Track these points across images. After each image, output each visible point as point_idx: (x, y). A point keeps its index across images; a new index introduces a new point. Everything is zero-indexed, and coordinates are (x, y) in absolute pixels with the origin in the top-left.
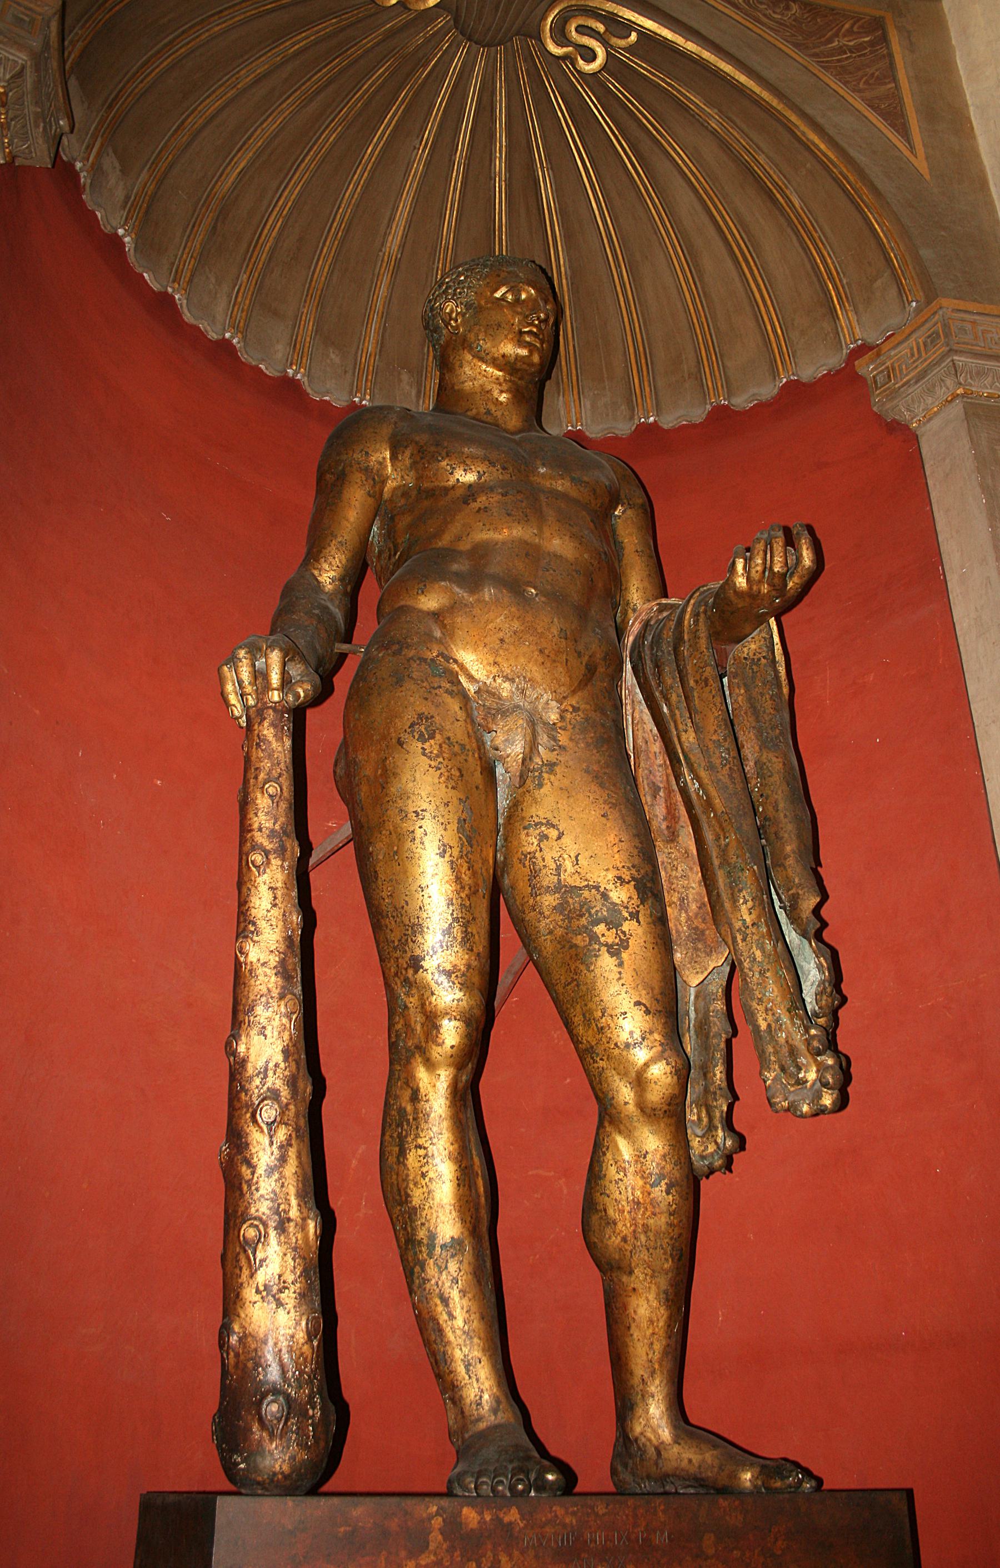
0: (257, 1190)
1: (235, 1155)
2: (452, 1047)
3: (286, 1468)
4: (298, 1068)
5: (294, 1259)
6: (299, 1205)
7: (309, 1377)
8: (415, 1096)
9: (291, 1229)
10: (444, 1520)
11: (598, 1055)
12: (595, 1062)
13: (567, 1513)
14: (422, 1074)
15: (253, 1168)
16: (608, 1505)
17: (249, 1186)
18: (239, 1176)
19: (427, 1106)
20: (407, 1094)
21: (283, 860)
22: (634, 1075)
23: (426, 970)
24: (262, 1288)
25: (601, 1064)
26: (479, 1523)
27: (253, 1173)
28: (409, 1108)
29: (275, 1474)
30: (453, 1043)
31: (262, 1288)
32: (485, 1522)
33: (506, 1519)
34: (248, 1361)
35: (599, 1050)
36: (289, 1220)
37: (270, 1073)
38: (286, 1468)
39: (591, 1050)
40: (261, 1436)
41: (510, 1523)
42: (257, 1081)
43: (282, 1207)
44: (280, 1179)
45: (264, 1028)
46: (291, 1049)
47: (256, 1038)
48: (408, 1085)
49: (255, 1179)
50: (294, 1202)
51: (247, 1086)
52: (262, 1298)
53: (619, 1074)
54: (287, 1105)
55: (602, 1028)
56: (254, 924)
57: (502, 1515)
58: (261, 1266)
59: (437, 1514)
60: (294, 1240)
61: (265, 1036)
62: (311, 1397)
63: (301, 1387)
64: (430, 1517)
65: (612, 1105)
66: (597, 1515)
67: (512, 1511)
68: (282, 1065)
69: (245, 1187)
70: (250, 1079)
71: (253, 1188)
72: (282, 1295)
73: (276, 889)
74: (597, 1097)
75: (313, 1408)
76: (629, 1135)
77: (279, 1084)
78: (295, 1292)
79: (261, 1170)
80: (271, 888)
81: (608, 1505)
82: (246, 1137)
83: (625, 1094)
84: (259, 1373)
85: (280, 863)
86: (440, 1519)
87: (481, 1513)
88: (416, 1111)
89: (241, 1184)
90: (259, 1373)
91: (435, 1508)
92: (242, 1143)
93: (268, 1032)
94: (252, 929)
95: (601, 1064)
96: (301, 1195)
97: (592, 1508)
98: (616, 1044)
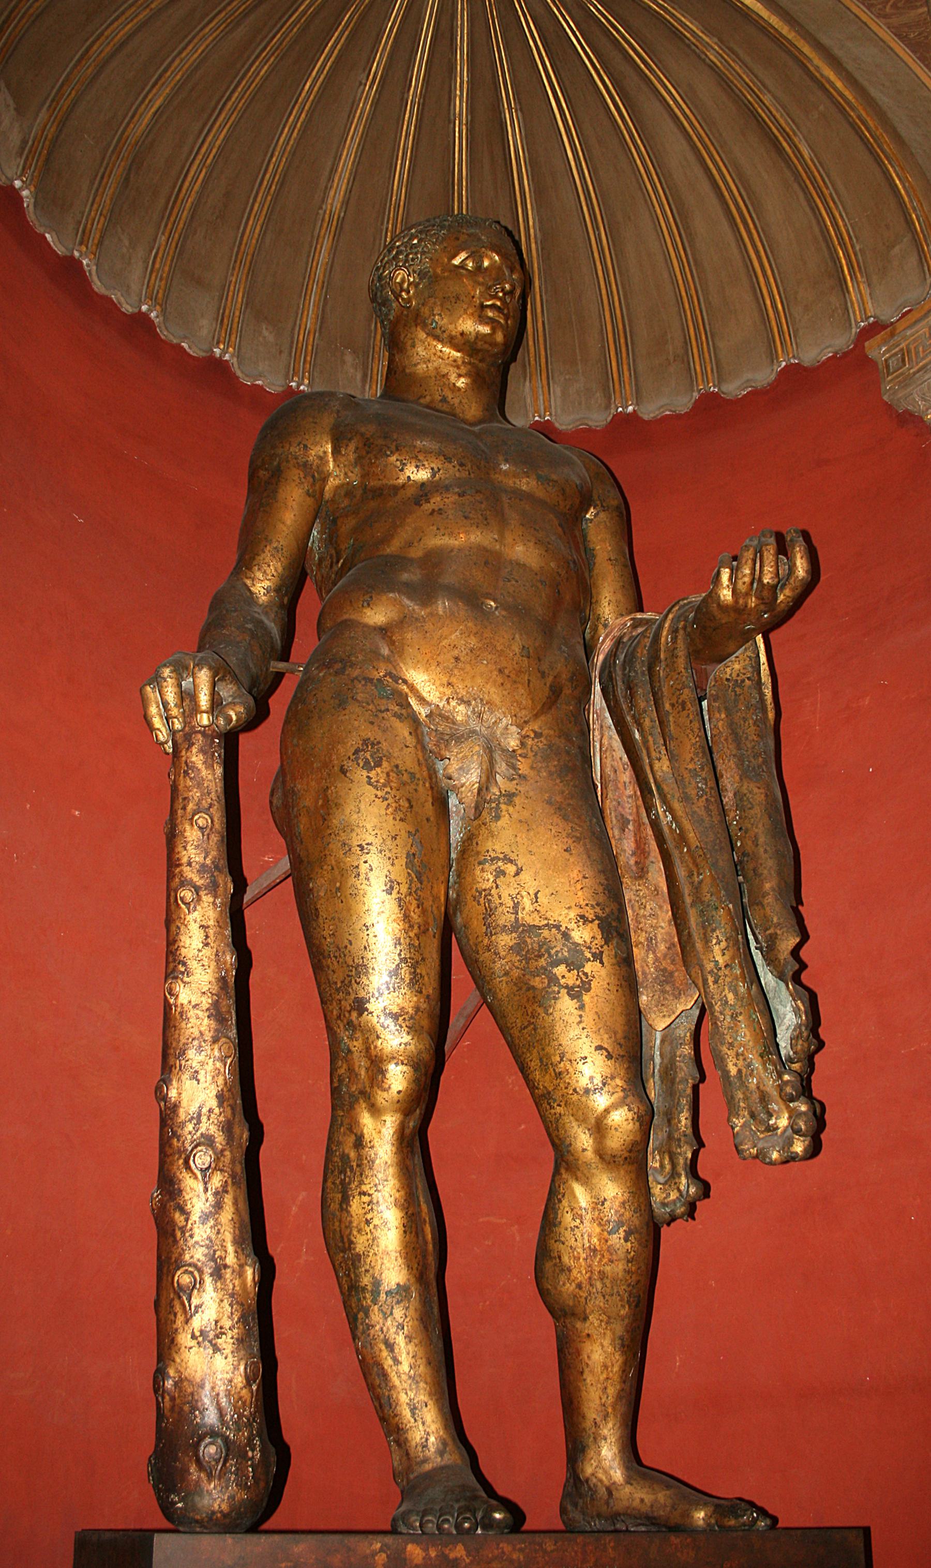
0: (192, 1236)
1: (168, 1201)
2: (399, 1092)
3: (225, 1507)
4: (233, 1114)
5: (231, 1305)
6: (236, 1252)
7: (248, 1420)
8: (359, 1142)
9: (228, 1276)
10: (388, 1557)
11: (555, 1100)
12: (552, 1107)
13: (514, 1549)
14: (366, 1121)
15: (187, 1214)
16: (556, 1542)
17: (183, 1233)
18: (172, 1223)
19: (372, 1152)
20: (351, 1139)
21: (215, 897)
22: (593, 1121)
23: (371, 1013)
24: (197, 1334)
25: (559, 1110)
26: (424, 1558)
27: (187, 1220)
28: (352, 1154)
29: (213, 1513)
30: (400, 1088)
31: (197, 1334)
32: (430, 1558)
33: (452, 1556)
34: (185, 1404)
35: (557, 1095)
36: (226, 1266)
37: (204, 1119)
38: (225, 1507)
39: (547, 1096)
40: (199, 1477)
41: (456, 1559)
42: (190, 1127)
43: (218, 1253)
44: (215, 1225)
45: (196, 1072)
46: (226, 1094)
47: (188, 1082)
48: (352, 1132)
49: (189, 1226)
50: (230, 1249)
51: (179, 1132)
52: (198, 1343)
53: (577, 1120)
54: (222, 1151)
55: (560, 1073)
56: (184, 964)
57: (447, 1552)
58: (197, 1312)
59: (381, 1550)
60: (231, 1287)
61: (198, 1081)
62: (250, 1439)
63: (240, 1430)
64: (374, 1554)
65: (569, 1152)
66: (545, 1552)
67: (458, 1548)
68: (217, 1111)
69: (179, 1234)
70: (183, 1125)
71: (187, 1234)
72: (219, 1341)
73: (208, 927)
74: (553, 1144)
75: (253, 1450)
76: (586, 1182)
77: (213, 1130)
78: (232, 1338)
79: (195, 1217)
80: (202, 926)
81: (556, 1542)
82: (179, 1184)
83: (583, 1140)
84: (196, 1417)
85: (211, 900)
86: (384, 1555)
87: (426, 1550)
88: (360, 1157)
89: (174, 1230)
90: (196, 1417)
91: (379, 1545)
92: (174, 1189)
93: (201, 1077)
94: (183, 969)
95: (559, 1110)
96: (238, 1242)
97: (540, 1545)
98: (575, 1090)
